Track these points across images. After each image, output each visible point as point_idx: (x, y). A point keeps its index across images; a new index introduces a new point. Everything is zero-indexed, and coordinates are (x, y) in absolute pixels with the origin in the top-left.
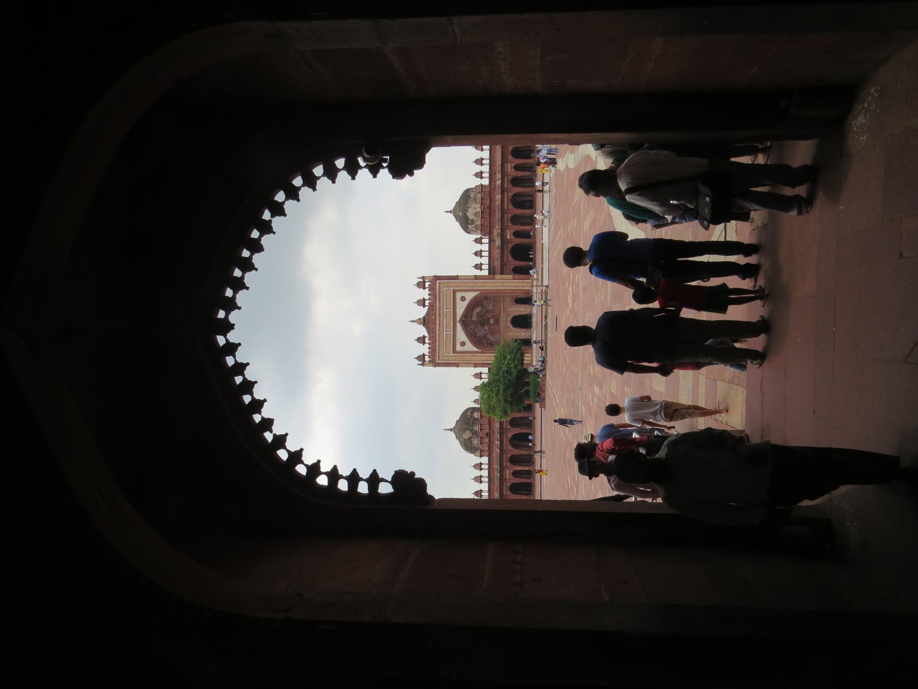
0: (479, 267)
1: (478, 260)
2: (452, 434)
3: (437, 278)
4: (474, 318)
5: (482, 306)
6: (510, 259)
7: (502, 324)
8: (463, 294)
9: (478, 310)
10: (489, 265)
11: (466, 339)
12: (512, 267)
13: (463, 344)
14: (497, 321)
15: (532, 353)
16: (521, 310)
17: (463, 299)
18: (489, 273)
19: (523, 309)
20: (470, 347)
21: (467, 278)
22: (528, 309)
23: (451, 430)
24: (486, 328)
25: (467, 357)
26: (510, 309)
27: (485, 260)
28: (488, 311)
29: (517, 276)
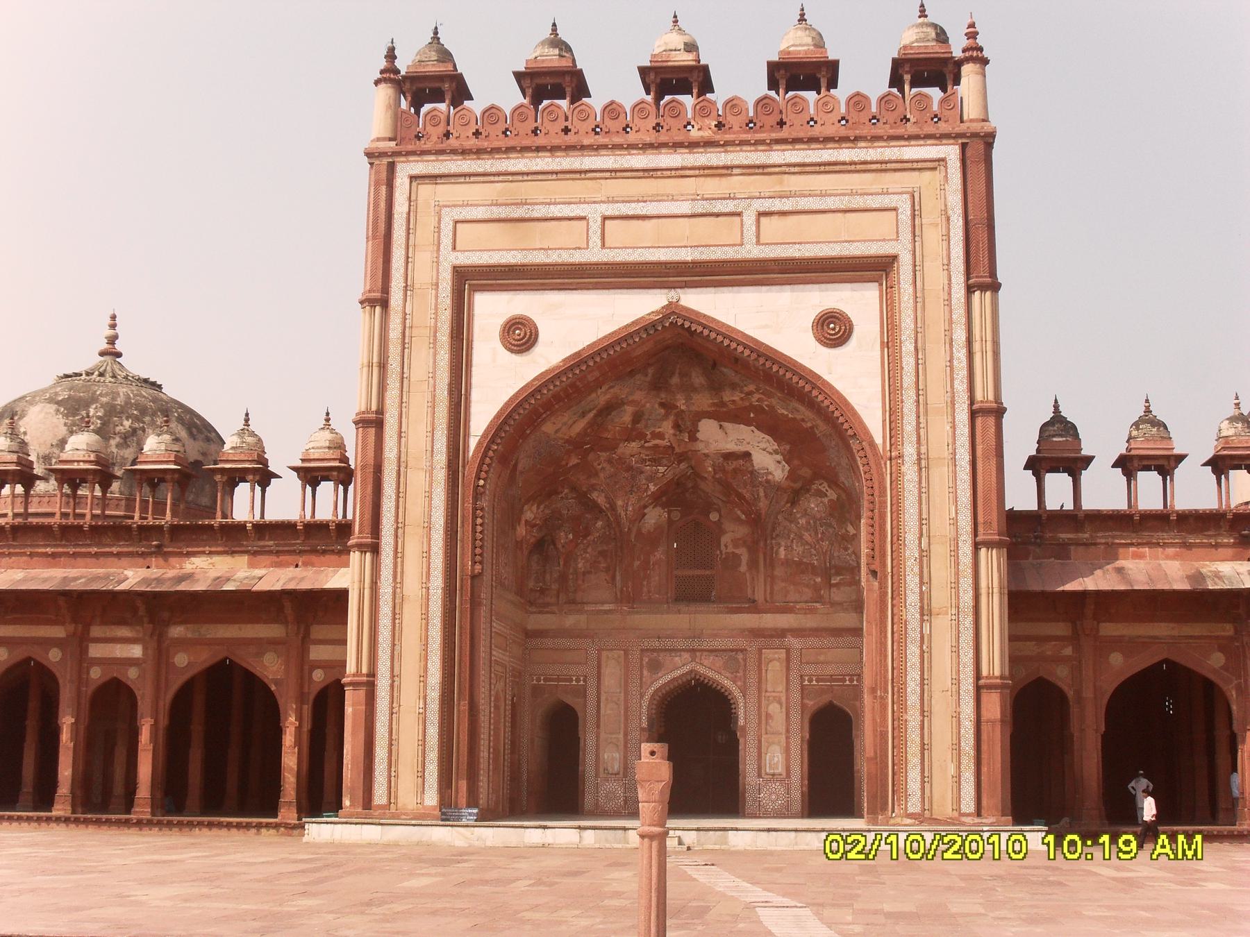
0: (1059, 451)
1: (1103, 440)
2: (87, 358)
3: (978, 147)
4: (717, 438)
5: (796, 491)
6: (1120, 666)
7: (679, 620)
8: (867, 326)
9: (768, 459)
10: (1077, 519)
11: (550, 354)
12: (1061, 675)
13: (520, 336)
14: (692, 593)
15: (447, 812)
16: (773, 753)
17: (833, 330)
18: (1015, 519)
19: (775, 759)
20: (499, 379)
21: (983, 348)
22: (772, 795)
23: (112, 353)
24: (654, 517)
25: (428, 365)
26: (774, 670)
27: (1103, 490)
28: (761, 530)
29: (994, 706)
